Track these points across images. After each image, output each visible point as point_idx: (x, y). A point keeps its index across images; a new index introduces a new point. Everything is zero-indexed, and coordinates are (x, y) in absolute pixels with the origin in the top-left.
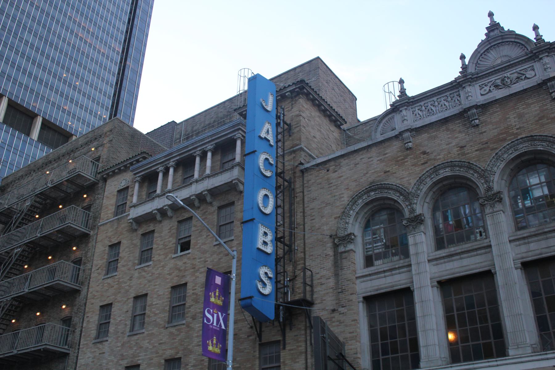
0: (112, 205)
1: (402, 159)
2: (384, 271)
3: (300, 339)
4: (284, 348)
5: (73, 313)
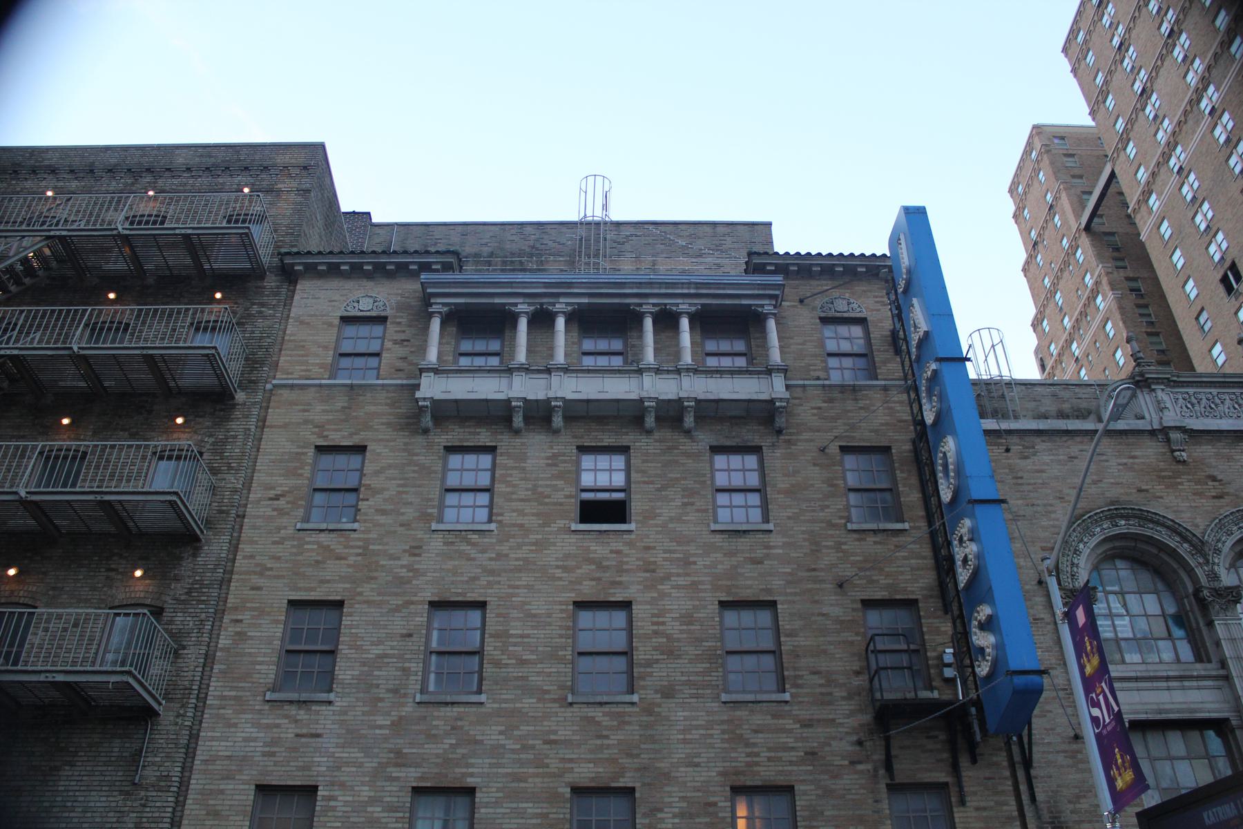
0: (326, 348)
1: (1170, 477)
2: (1168, 678)
3: (1000, 788)
4: (963, 803)
5: (168, 599)
